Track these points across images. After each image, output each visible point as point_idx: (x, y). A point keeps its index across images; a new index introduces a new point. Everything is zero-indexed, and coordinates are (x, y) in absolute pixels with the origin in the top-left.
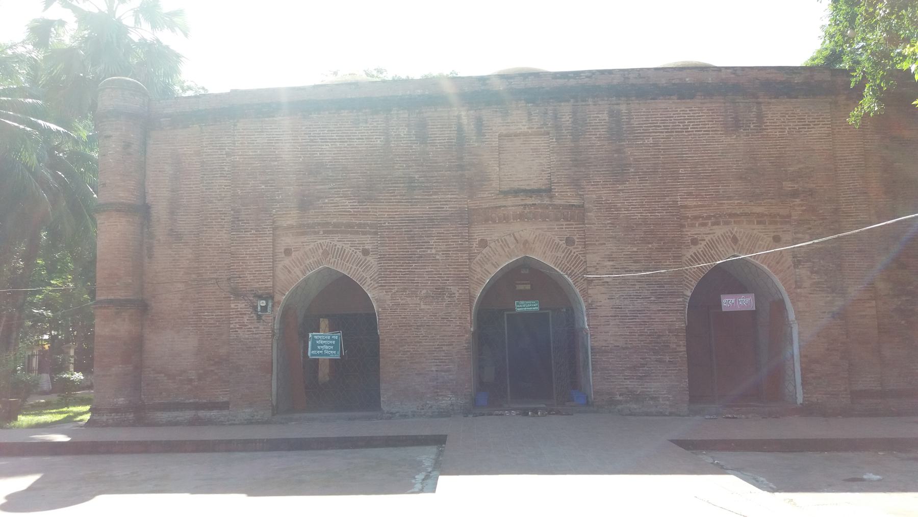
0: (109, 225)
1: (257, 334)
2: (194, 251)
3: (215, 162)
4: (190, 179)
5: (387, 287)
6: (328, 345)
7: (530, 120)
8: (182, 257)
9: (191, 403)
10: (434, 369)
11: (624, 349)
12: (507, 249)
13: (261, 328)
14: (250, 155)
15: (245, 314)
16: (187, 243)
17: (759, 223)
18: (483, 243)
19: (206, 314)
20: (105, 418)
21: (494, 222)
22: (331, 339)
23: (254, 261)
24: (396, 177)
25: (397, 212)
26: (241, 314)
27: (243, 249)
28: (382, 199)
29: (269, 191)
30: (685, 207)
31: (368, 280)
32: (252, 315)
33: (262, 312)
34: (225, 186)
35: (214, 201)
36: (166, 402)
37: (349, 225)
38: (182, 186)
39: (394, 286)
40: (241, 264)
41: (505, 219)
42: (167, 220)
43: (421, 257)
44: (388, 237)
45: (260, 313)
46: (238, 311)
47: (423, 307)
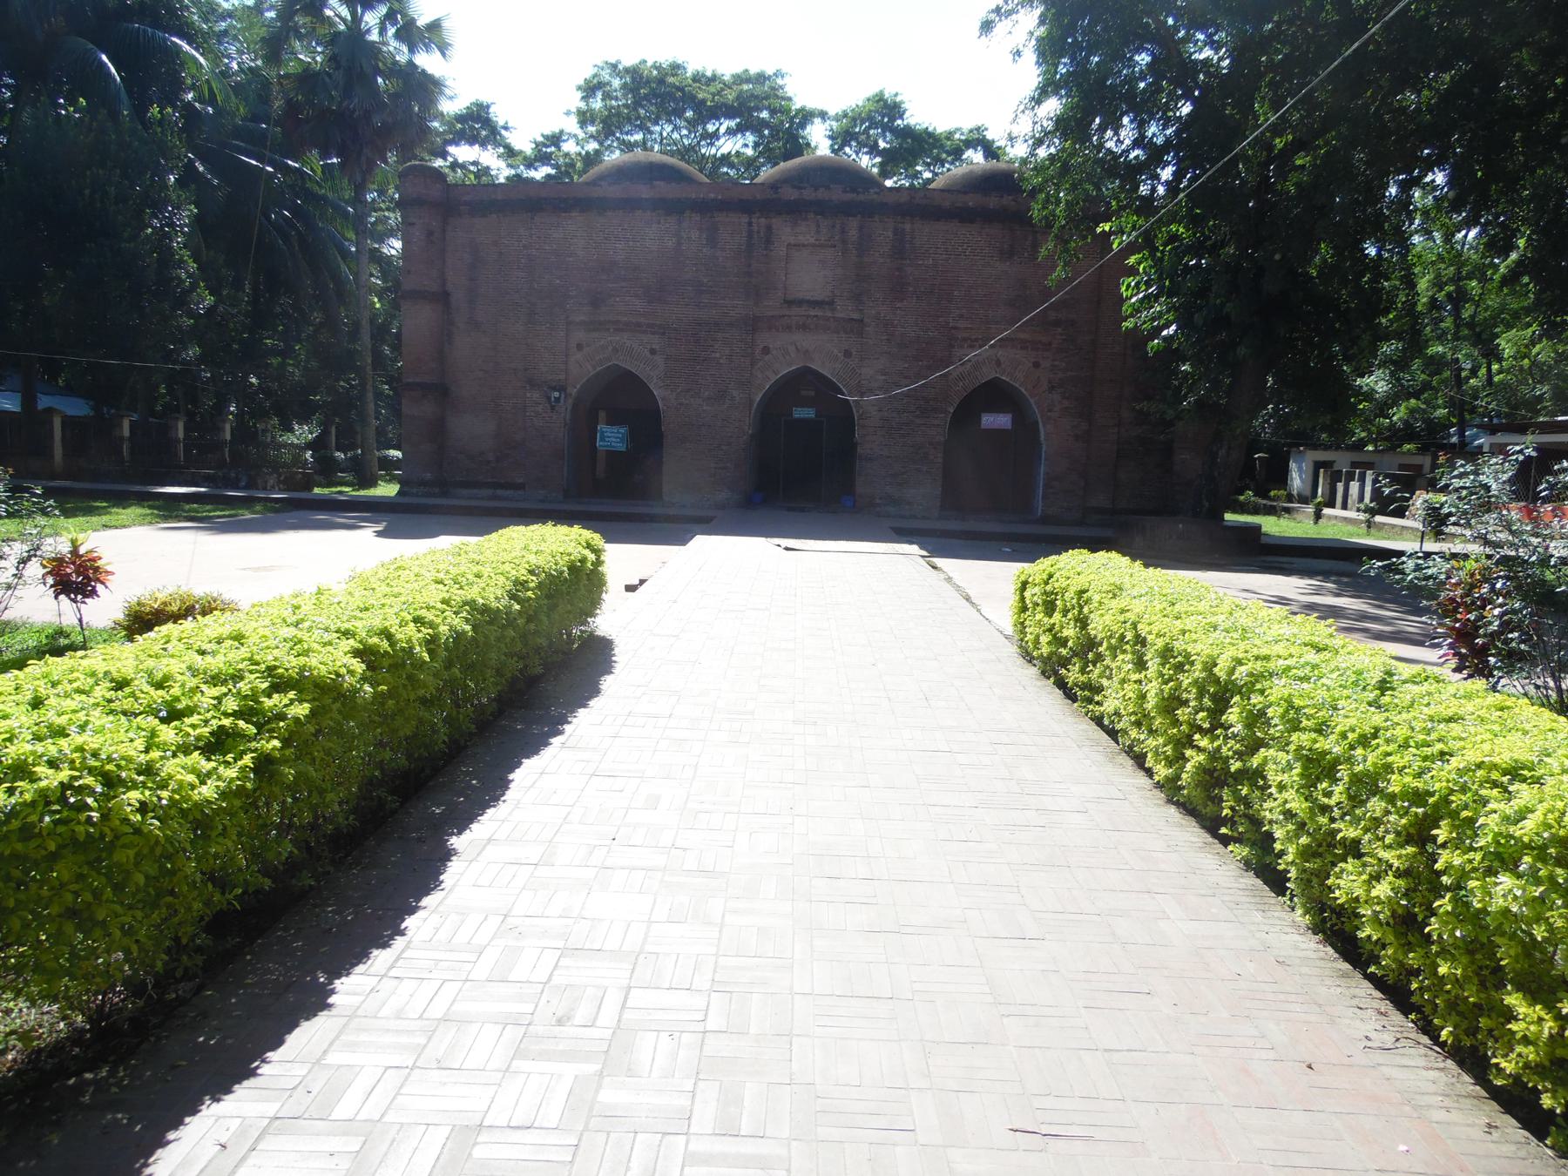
7: (818, 232)
12: (788, 357)
18: (766, 350)
20: (415, 490)
21: (778, 330)
22: (618, 432)
30: (955, 328)
37: (639, 325)
41: (789, 328)
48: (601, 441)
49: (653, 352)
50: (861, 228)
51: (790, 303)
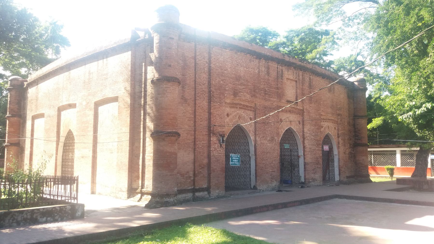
0: (173, 90)
1: (220, 153)
2: (192, 109)
3: (202, 65)
4: (190, 70)
5: (259, 135)
6: (236, 160)
7: (293, 75)
8: (187, 111)
9: (190, 189)
10: (271, 171)
11: (312, 163)
14: (217, 65)
15: (216, 143)
16: (189, 104)
17: (333, 123)
19: (199, 142)
20: (172, 200)
22: (237, 157)
23: (219, 118)
24: (261, 88)
25: (261, 103)
26: (215, 143)
27: (215, 111)
28: (258, 97)
29: (224, 85)
30: (322, 115)
31: (251, 131)
32: (219, 144)
33: (222, 143)
34: (205, 78)
35: (201, 85)
36: (180, 189)
37: (247, 106)
38: (187, 73)
39: (260, 135)
40: (215, 118)
42: (181, 90)
43: (268, 124)
44: (259, 114)
45: (221, 144)
46: (214, 142)
47: (268, 145)
48: (232, 161)
50: (302, 75)
51: (289, 102)
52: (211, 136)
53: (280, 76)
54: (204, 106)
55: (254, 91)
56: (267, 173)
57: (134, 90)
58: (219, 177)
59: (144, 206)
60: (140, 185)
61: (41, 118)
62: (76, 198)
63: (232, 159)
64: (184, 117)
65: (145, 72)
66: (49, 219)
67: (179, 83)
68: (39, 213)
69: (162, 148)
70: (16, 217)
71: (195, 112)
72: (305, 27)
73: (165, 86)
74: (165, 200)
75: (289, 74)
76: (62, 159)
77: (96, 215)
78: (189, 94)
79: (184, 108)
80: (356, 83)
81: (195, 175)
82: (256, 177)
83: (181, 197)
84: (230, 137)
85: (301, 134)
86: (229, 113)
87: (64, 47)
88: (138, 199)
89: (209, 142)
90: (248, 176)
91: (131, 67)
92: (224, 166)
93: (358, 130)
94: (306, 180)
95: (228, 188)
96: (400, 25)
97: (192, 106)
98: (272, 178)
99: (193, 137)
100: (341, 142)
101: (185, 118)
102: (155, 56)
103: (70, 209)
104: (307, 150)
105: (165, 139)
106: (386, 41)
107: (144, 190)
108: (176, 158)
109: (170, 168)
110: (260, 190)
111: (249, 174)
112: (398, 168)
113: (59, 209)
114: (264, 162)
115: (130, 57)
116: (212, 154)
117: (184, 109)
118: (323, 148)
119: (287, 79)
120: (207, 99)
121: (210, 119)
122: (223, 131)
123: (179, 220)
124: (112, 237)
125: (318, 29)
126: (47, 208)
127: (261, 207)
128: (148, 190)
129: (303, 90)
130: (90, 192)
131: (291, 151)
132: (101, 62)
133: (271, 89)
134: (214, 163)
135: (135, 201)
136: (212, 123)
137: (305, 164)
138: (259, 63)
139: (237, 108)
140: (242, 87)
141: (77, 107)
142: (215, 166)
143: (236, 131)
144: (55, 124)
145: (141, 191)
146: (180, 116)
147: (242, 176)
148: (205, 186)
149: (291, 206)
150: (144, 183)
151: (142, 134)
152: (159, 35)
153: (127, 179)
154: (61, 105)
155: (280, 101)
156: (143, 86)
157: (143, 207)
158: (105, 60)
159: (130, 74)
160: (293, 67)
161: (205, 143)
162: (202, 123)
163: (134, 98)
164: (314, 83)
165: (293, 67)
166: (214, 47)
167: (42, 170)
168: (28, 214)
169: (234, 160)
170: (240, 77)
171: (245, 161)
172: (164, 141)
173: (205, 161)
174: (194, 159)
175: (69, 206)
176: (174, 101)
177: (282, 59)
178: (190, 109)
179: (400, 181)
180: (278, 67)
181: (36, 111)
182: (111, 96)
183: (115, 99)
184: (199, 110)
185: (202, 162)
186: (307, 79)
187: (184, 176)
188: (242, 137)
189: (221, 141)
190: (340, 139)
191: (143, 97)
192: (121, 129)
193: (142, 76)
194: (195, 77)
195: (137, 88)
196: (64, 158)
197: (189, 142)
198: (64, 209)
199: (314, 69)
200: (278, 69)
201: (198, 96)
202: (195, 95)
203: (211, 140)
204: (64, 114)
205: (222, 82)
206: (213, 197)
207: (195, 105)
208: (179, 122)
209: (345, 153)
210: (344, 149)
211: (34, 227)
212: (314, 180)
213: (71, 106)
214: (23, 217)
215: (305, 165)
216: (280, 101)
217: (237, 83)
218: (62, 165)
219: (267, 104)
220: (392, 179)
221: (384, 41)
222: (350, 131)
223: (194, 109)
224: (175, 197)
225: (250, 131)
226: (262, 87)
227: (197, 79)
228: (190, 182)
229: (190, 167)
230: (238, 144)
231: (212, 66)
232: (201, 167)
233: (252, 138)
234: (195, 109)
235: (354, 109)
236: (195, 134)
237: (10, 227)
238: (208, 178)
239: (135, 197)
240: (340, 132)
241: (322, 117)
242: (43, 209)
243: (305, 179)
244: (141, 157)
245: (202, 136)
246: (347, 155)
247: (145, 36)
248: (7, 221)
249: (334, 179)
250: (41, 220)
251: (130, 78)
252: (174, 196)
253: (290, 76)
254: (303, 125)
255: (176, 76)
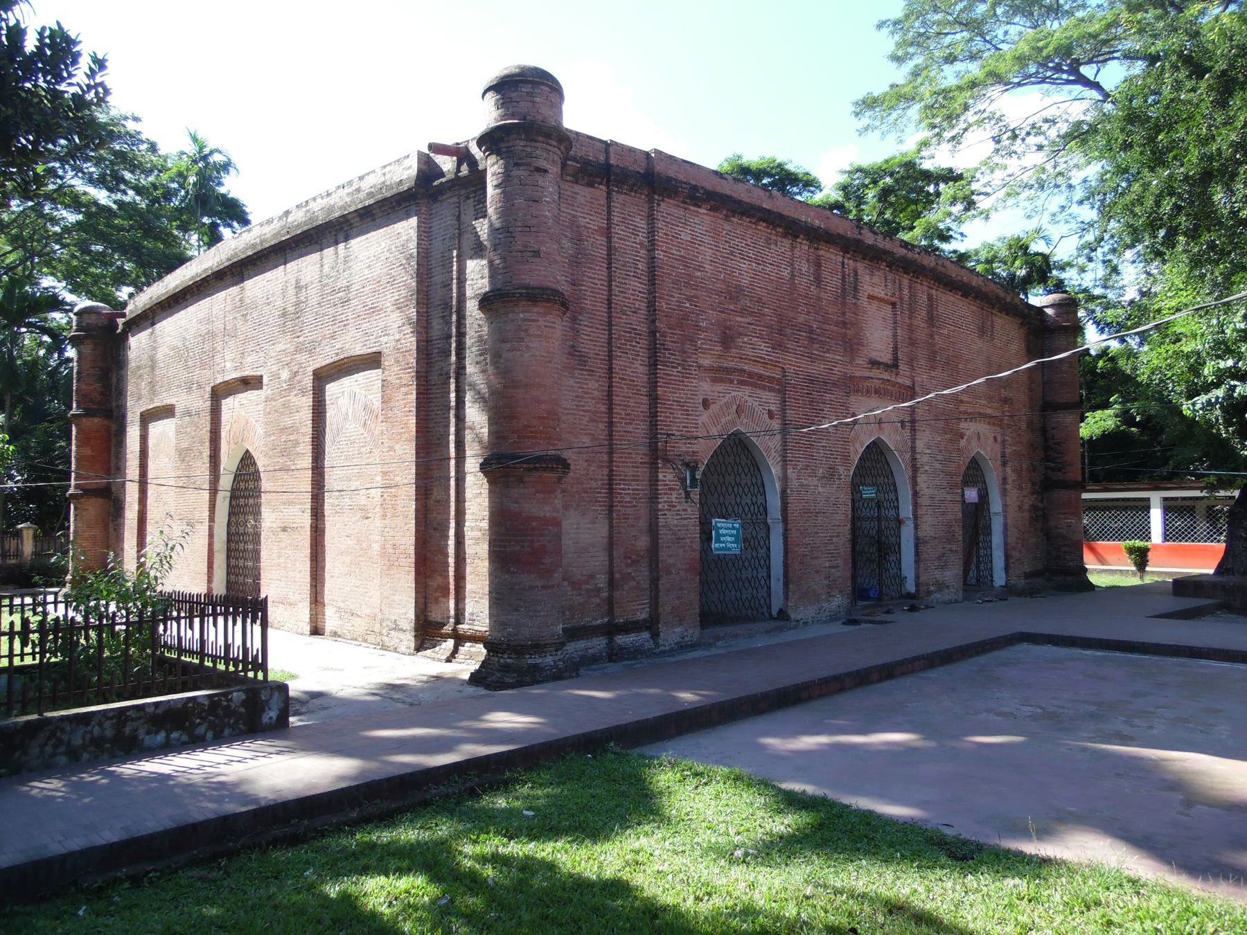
1: (685, 519)
2: (600, 385)
6: (730, 536)
8: (587, 393)
10: (827, 565)
11: (935, 538)
13: (689, 510)
15: (673, 489)
16: (593, 371)
17: (989, 423)
22: (733, 528)
23: (680, 412)
26: (670, 489)
30: (961, 401)
31: (773, 451)
36: (569, 626)
37: (760, 377)
42: (567, 329)
47: (821, 490)
48: (718, 541)
49: (771, 415)
50: (910, 287)
51: (874, 363)
52: (658, 468)
53: (849, 288)
54: (636, 377)
55: (781, 332)
56: (817, 572)
57: (427, 333)
58: (682, 589)
59: (466, 676)
60: (452, 613)
61: (167, 417)
62: (263, 667)
63: (717, 533)
64: (579, 410)
65: (458, 279)
66: (175, 735)
67: (565, 305)
68: (142, 721)
69: (516, 505)
70: (65, 738)
71: (610, 395)
72: (895, 158)
73: (521, 315)
74: (530, 661)
75: (874, 283)
76: (228, 534)
77: (324, 709)
78: (591, 340)
79: (577, 383)
80: (1050, 311)
81: (612, 583)
82: (786, 584)
83: (575, 648)
84: (712, 468)
85: (908, 456)
86: (709, 398)
87: (230, 226)
88: (448, 653)
89: (651, 485)
90: (763, 582)
91: (418, 264)
92: (696, 555)
93: (1054, 444)
94: (921, 589)
95: (708, 618)
96: (1198, 135)
97: (600, 377)
98: (829, 586)
99: (606, 472)
100: (1012, 477)
101: (582, 413)
102: (491, 225)
103: (243, 701)
104: (924, 501)
105: (526, 479)
106: (1154, 183)
107: (464, 627)
108: (558, 536)
109: (542, 566)
110: (797, 621)
111: (765, 575)
112: (1155, 546)
113: (206, 703)
114: (808, 540)
115: (413, 234)
116: (662, 521)
117: (579, 387)
118: (963, 495)
119: (871, 297)
120: (644, 354)
121: (653, 415)
122: (694, 452)
123: (583, 735)
124: (379, 801)
125: (927, 165)
126: (169, 701)
127: (825, 682)
128: (476, 628)
129: (911, 329)
130: (307, 629)
131: (879, 507)
132: (329, 252)
133: (827, 327)
134: (669, 547)
135: (439, 660)
136: (662, 429)
137: (918, 543)
138: (793, 248)
139: (731, 381)
140: (746, 320)
141: (265, 387)
142: (670, 556)
143: (729, 449)
144: (207, 437)
145: (455, 630)
146: (566, 409)
147: (747, 585)
148: (642, 615)
149: (903, 674)
150: (464, 609)
151: (453, 462)
152: (501, 162)
153: (414, 596)
154: (219, 380)
155: (851, 362)
156: (454, 317)
157: (464, 681)
158: (341, 246)
159: (414, 284)
160: (884, 264)
161: (642, 490)
162: (630, 428)
163: (428, 355)
164: (941, 309)
165: (884, 264)
166: (663, 200)
167: (158, 575)
168: (107, 724)
169: (724, 536)
170: (740, 289)
171: (755, 539)
172: (522, 485)
173: (643, 542)
174: (611, 537)
175: (239, 691)
176: (550, 362)
177: (854, 239)
178: (595, 386)
179: (1183, 586)
180: (846, 261)
181: (152, 400)
182: (361, 352)
183: (372, 361)
184: (621, 388)
185: (632, 545)
186: (923, 298)
187: (580, 588)
188: (746, 470)
189: (688, 482)
190: (1008, 470)
191: (453, 353)
192: (391, 449)
193: (451, 289)
194: (610, 290)
195: (436, 324)
196: (233, 530)
197: (595, 485)
198: (225, 703)
199: (940, 268)
200: (843, 267)
201: (619, 348)
202: (610, 343)
203: (658, 481)
204: (228, 404)
205: (688, 305)
206: (667, 648)
207: (612, 373)
208: (563, 426)
209: (1020, 507)
210: (1018, 498)
211: (128, 769)
212: (941, 586)
213: (249, 383)
214: (88, 736)
215: (917, 546)
216: (851, 362)
217: (732, 307)
218: (228, 550)
219: (817, 369)
220: (1141, 578)
221: (1146, 186)
222: (1032, 445)
223: (607, 385)
224: (559, 653)
225: (768, 450)
226: (801, 319)
227: (616, 295)
228: (598, 605)
229: (598, 561)
230: (736, 489)
231: (659, 254)
232: (629, 561)
233: (775, 470)
234: (610, 386)
235: (1044, 383)
236: (611, 461)
237: (47, 770)
238: (651, 592)
239: (437, 648)
240: (1008, 451)
241: (962, 408)
242: (157, 704)
243: (917, 585)
244: (452, 532)
245: (633, 467)
246: (1027, 515)
247: (458, 170)
248: (35, 751)
249: (992, 581)
250: (148, 740)
251: (415, 297)
252: (556, 650)
253: (876, 290)
254: (913, 430)
255: (554, 286)
